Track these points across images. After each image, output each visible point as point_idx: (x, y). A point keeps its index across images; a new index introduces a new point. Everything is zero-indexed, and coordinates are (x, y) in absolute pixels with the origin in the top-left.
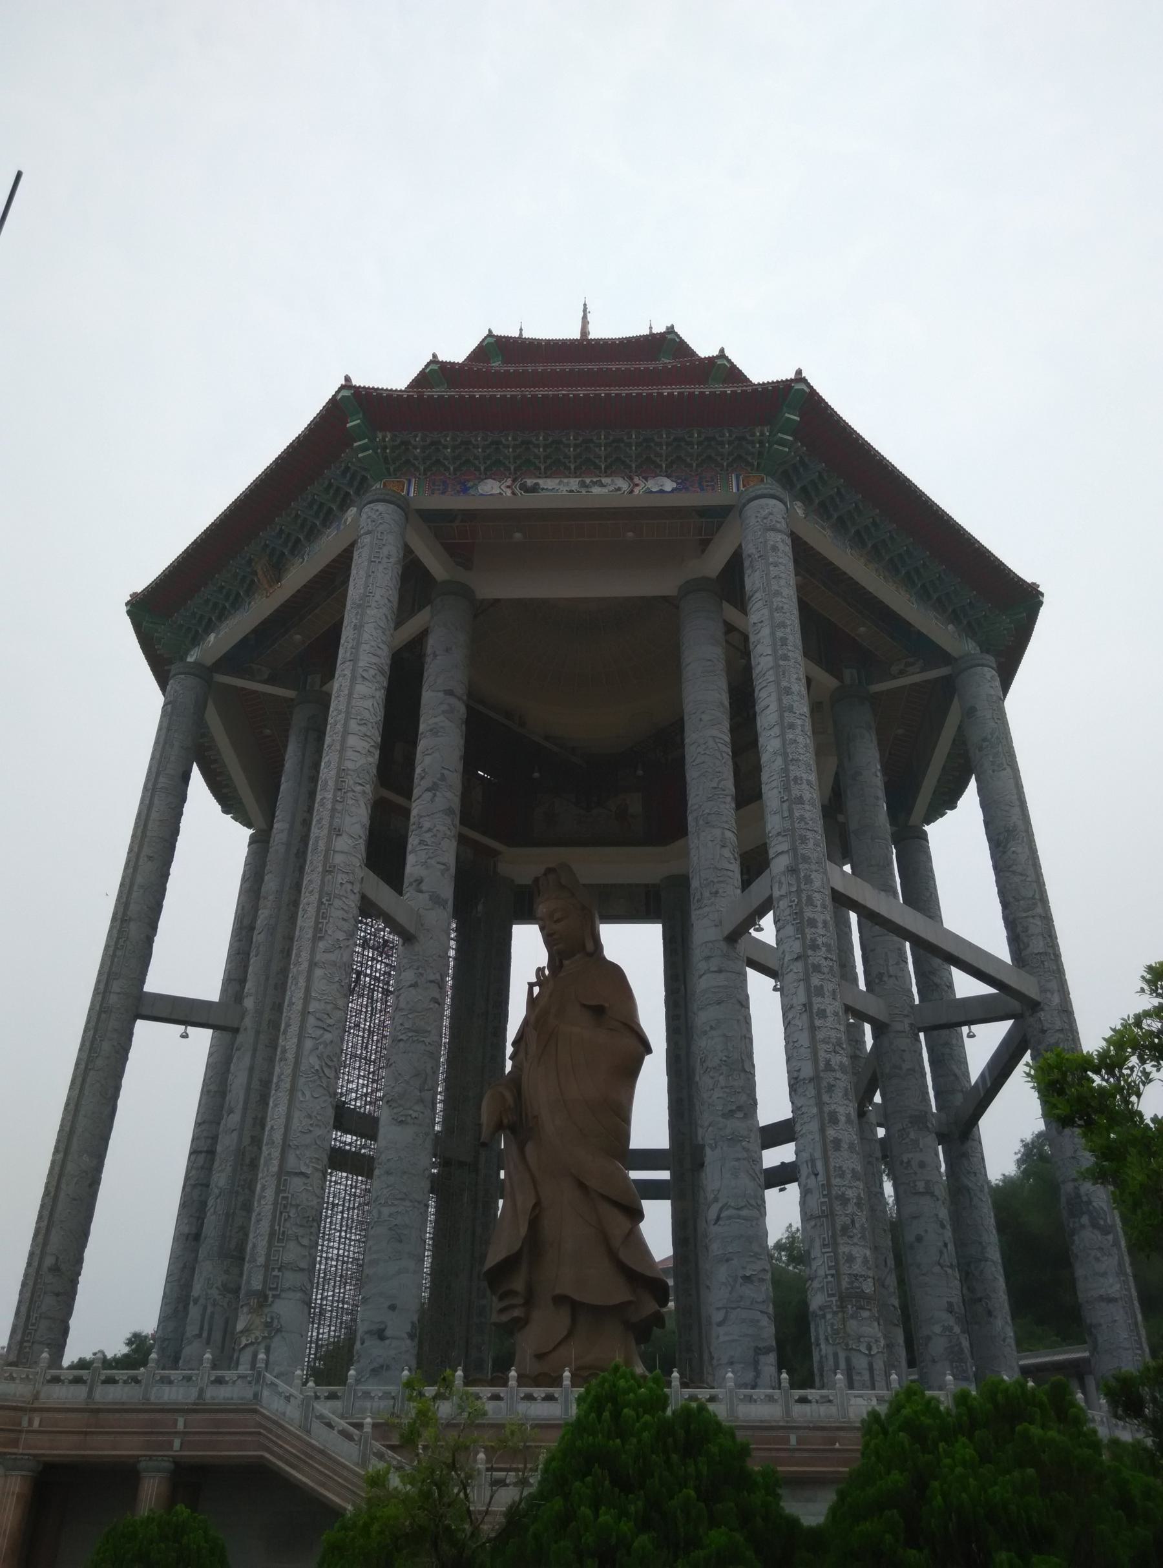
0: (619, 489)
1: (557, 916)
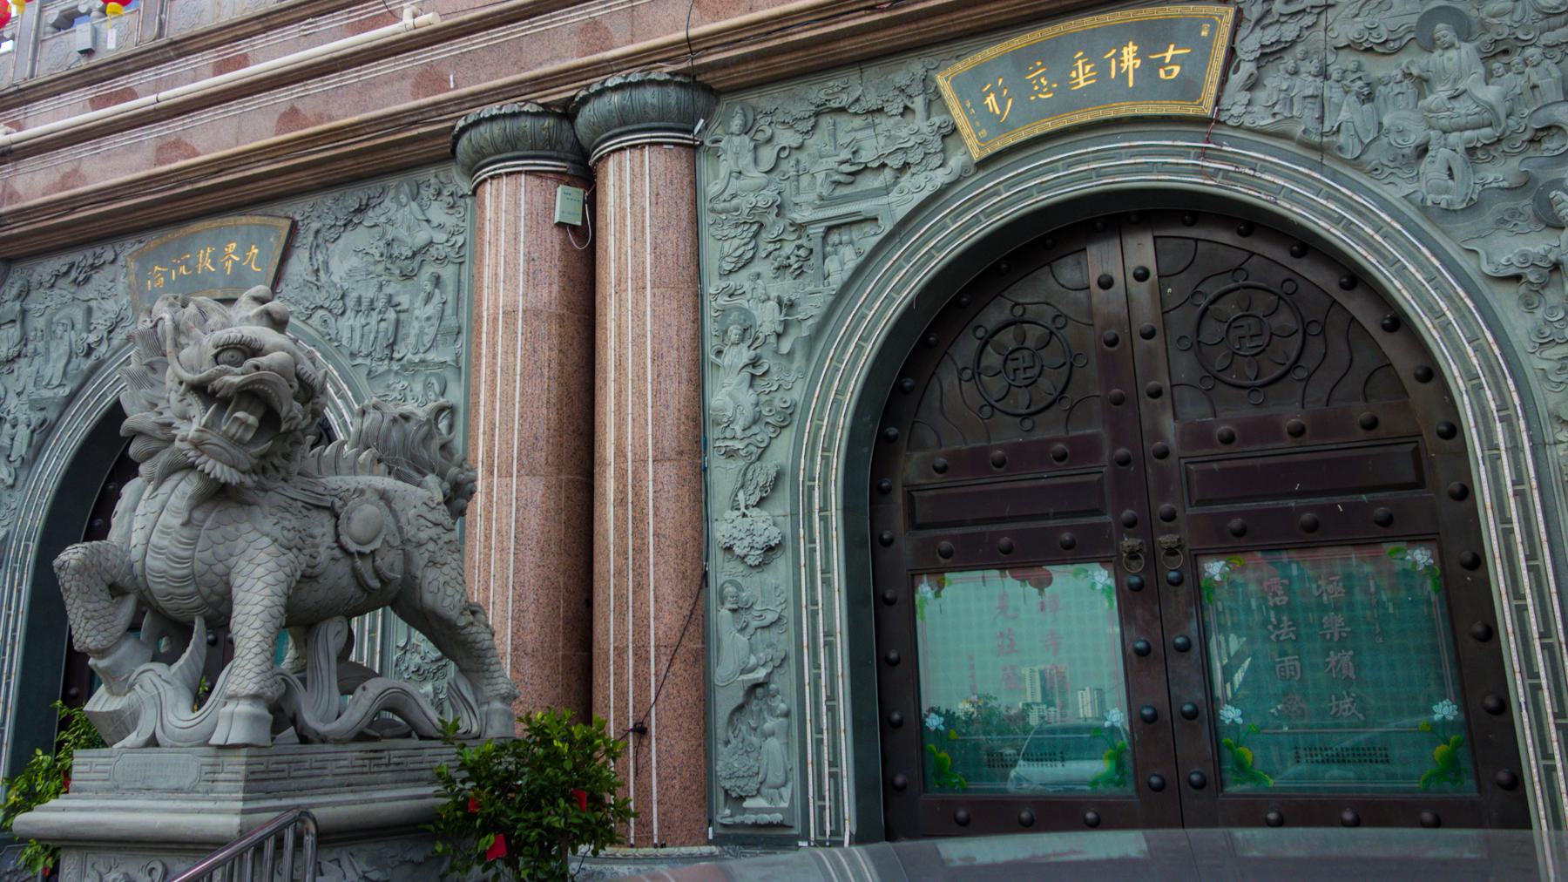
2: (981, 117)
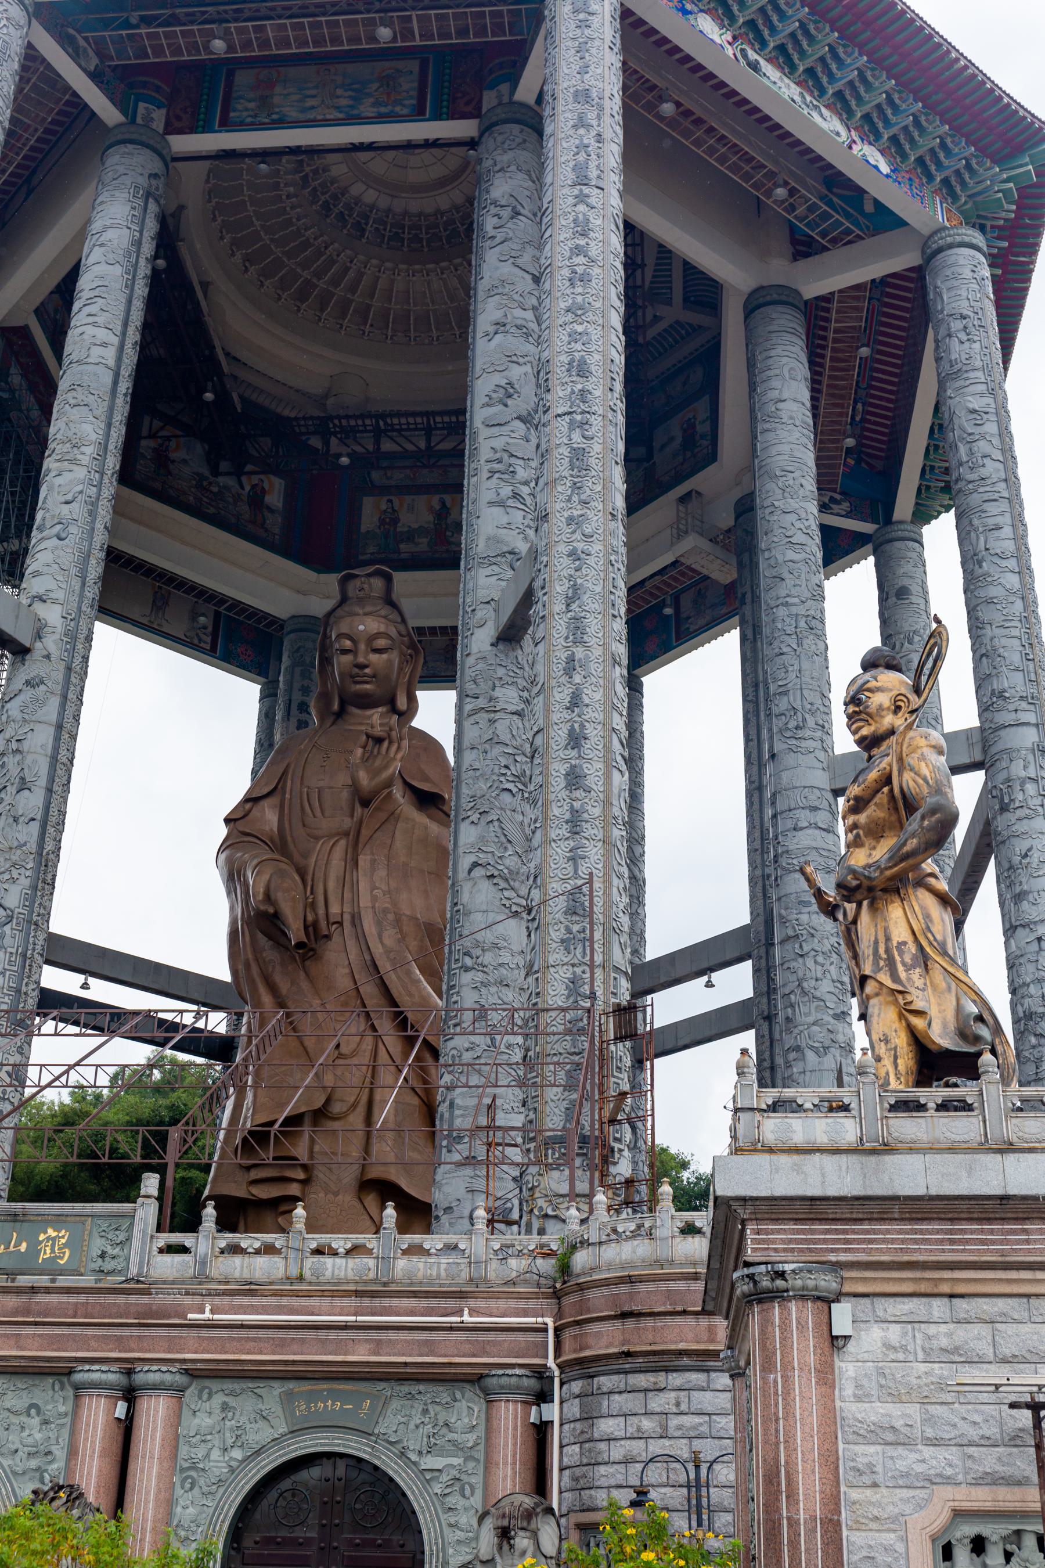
0: (838, 134)
1: (381, 643)
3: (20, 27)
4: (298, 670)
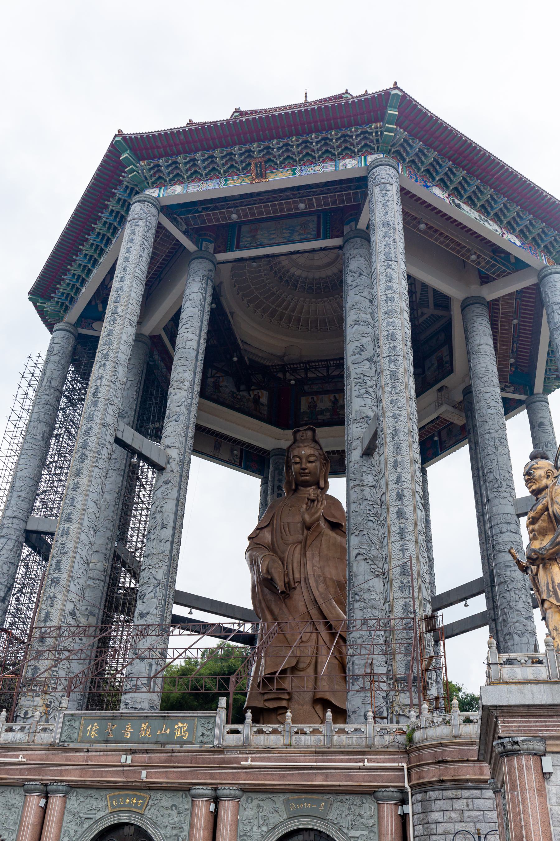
0: (497, 231)
1: (312, 458)
2: (112, 805)
3: (154, 216)
4: (277, 472)
